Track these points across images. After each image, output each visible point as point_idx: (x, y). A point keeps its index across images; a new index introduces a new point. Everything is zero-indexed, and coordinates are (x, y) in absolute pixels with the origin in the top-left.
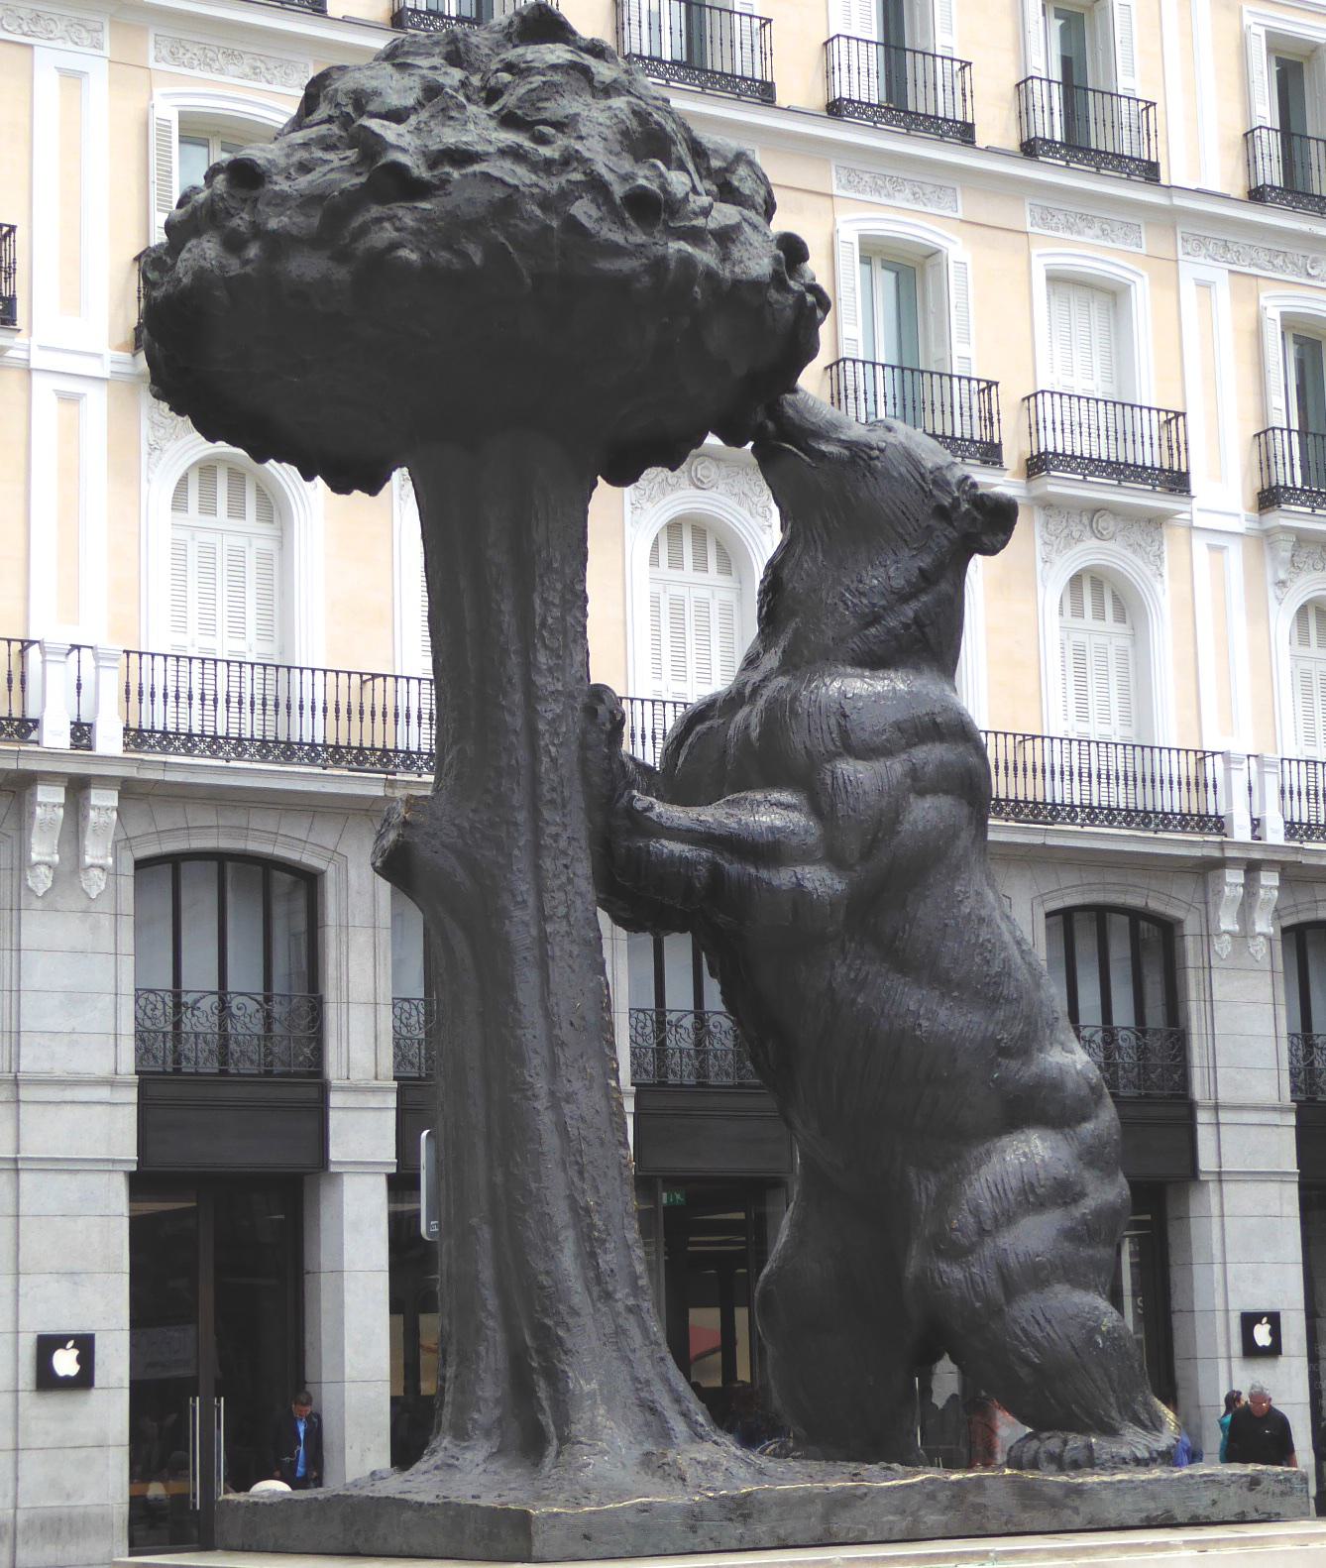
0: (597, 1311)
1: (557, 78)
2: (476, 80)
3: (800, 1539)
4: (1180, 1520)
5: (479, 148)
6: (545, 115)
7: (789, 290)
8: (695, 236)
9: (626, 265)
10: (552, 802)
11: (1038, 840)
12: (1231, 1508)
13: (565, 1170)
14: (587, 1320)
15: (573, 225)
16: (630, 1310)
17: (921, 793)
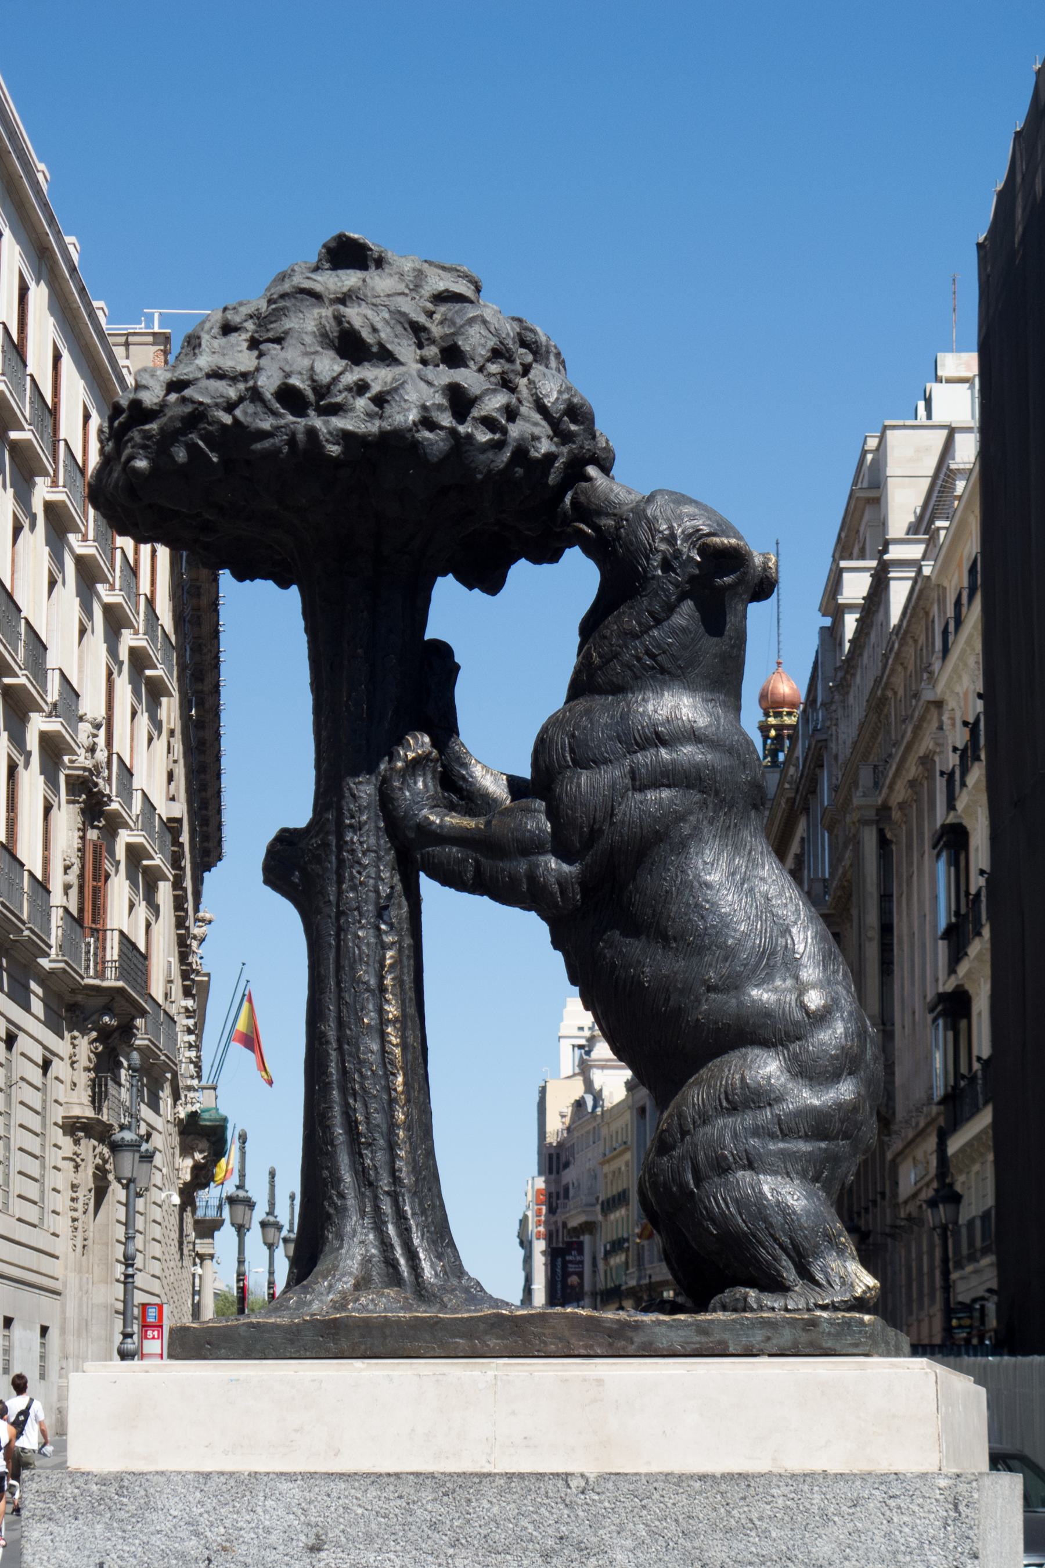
4: (731, 1350)
5: (191, 377)
6: (270, 335)
9: (266, 444)
10: (351, 826)
14: (351, 1202)
16: (388, 1193)
17: (642, 789)
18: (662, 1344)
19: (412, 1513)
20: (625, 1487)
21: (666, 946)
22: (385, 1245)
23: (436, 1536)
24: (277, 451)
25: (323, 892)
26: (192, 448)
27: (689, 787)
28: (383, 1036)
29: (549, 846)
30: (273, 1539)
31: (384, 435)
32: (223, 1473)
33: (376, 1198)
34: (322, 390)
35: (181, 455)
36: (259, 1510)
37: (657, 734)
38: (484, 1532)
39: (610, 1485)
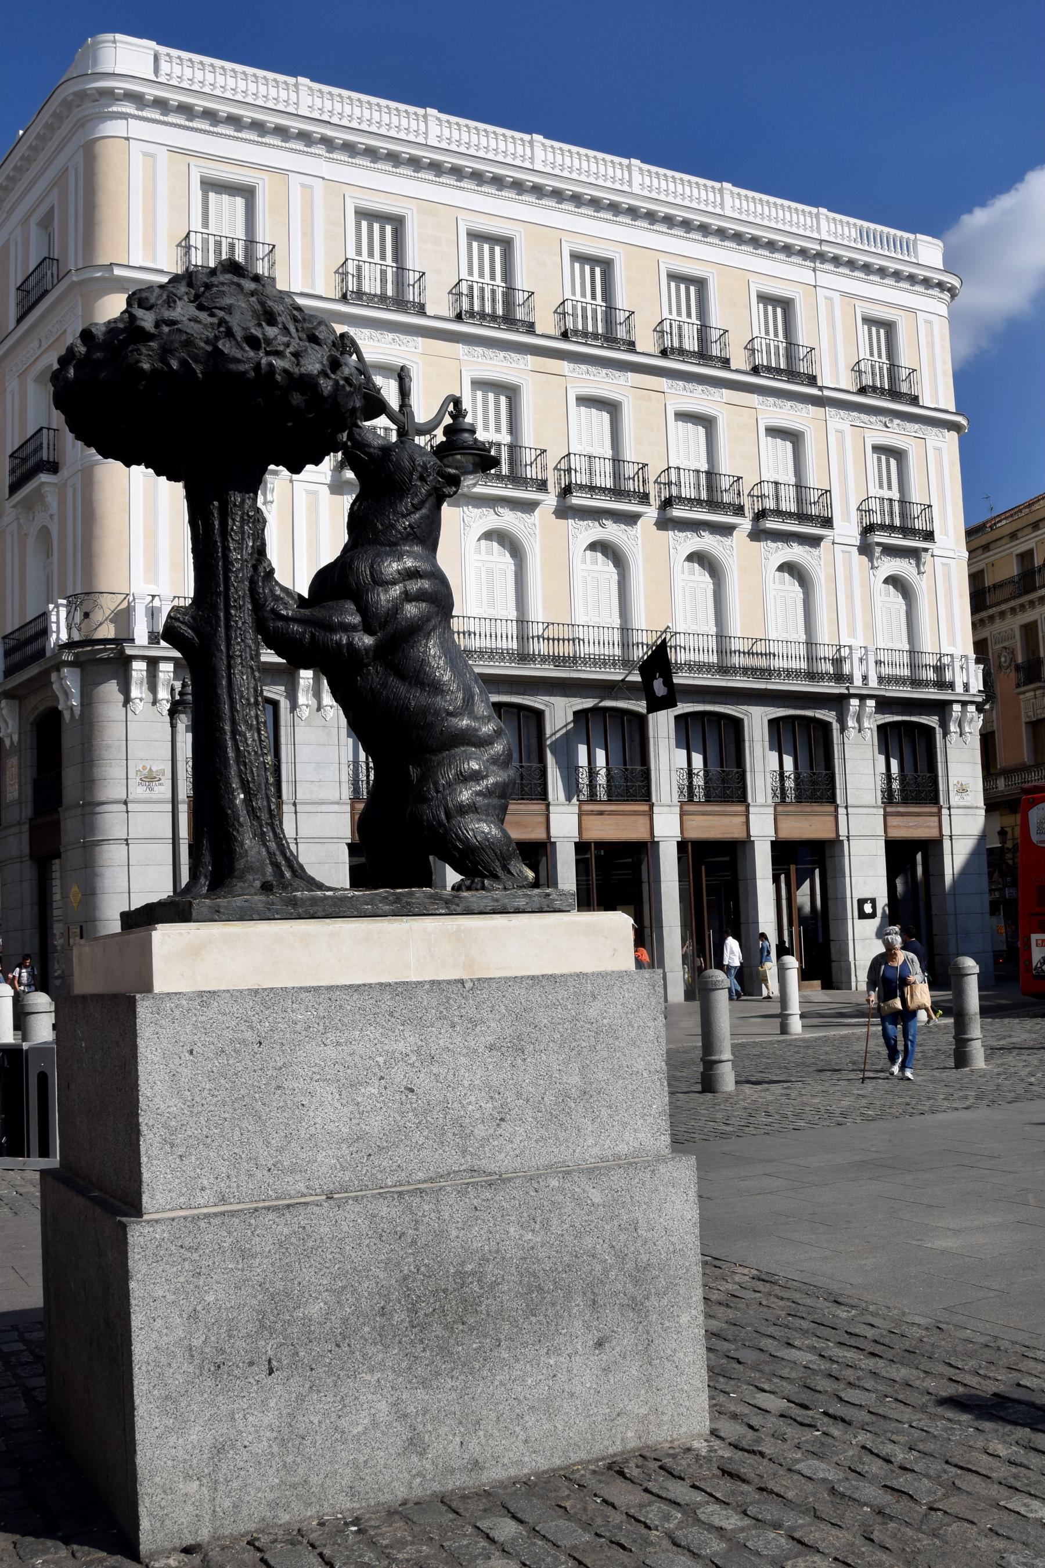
0: (252, 824)
1: (225, 288)
2: (193, 292)
3: (319, 914)
7: (330, 378)
8: (278, 354)
9: (242, 368)
11: (762, 686)
12: (536, 906)
13: (238, 765)
15: (217, 351)
16: (267, 824)
18: (475, 907)
19: (379, 1007)
20: (494, 986)
21: (423, 689)
22: (271, 854)
23: (393, 1020)
24: (244, 373)
25: (218, 646)
26: (183, 363)
27: (433, 602)
28: (259, 731)
29: (360, 628)
30: (298, 1028)
31: (302, 375)
32: (266, 989)
33: (261, 826)
34: (268, 341)
35: (175, 364)
36: (289, 1010)
37: (418, 572)
38: (419, 1015)
39: (486, 985)
